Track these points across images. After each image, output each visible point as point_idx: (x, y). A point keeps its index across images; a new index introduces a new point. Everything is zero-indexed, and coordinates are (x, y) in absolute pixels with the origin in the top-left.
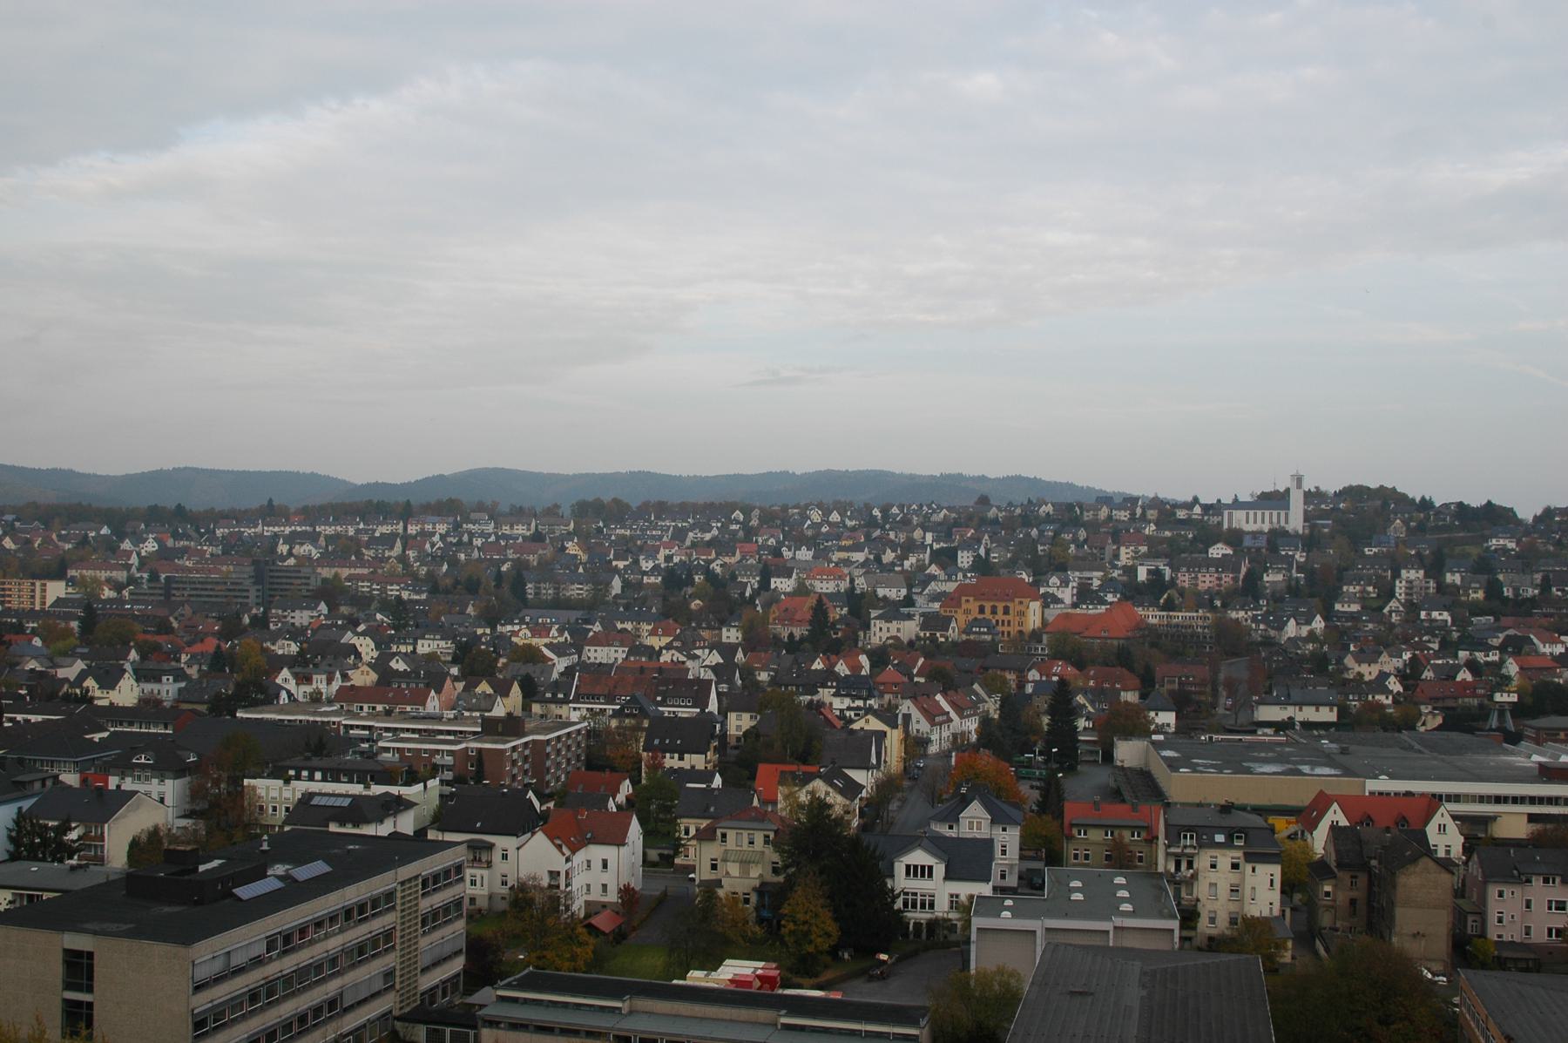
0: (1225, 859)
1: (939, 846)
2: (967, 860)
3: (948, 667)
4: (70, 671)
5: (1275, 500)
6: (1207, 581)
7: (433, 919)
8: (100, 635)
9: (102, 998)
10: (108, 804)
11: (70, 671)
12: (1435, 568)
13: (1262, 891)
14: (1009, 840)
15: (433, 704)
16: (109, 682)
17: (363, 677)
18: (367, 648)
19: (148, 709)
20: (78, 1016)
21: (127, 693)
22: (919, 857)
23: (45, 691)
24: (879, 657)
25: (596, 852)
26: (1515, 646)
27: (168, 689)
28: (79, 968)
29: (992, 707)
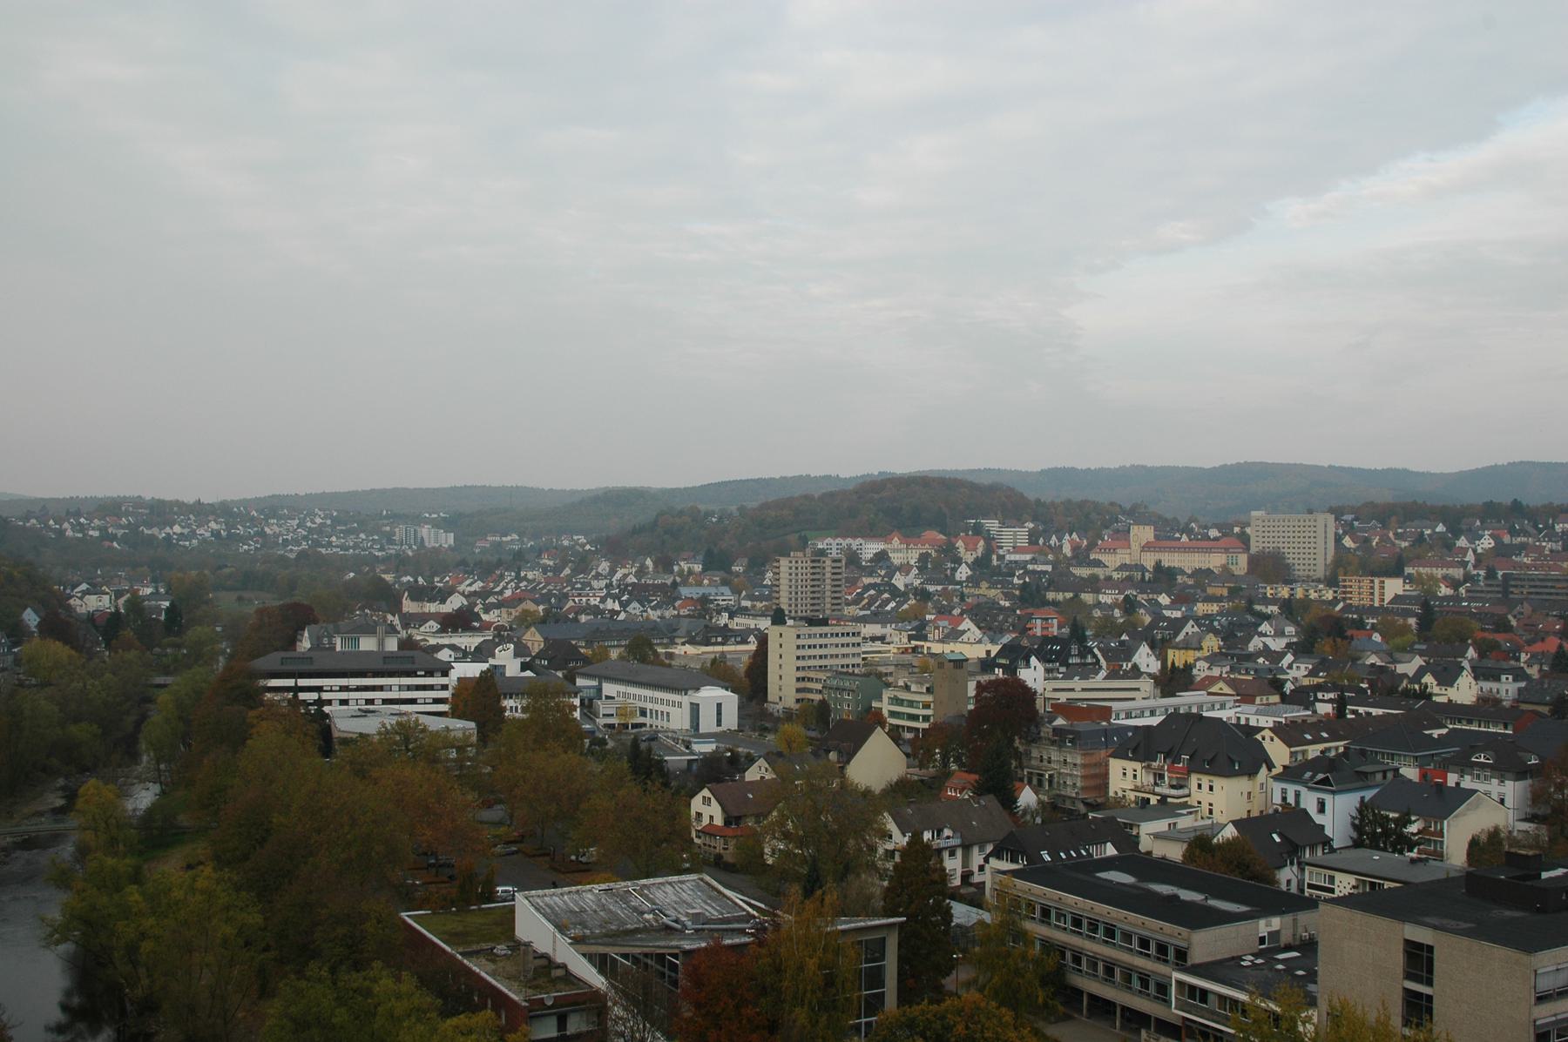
4: (1409, 667)
8: (1440, 634)
9: (1439, 991)
10: (1449, 801)
11: (1409, 667)
16: (1448, 677)
19: (1487, 707)
20: (1418, 1008)
21: (1465, 690)
23: (1385, 686)
27: (1507, 688)
28: (1419, 960)
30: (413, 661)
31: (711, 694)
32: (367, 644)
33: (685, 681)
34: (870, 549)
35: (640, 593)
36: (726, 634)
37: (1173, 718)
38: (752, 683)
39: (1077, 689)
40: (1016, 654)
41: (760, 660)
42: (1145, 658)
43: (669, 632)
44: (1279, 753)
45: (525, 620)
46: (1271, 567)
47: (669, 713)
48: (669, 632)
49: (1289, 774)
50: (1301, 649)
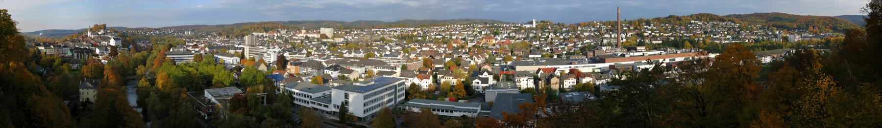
1: (480, 79)
3: (479, 50)
6: (521, 36)
7: (400, 90)
12: (555, 33)
13: (531, 84)
17: (388, 53)
18: (388, 48)
21: (353, 55)
22: (477, 80)
24: (470, 49)
25: (425, 80)
26: (566, 45)
29: (487, 56)
30: (188, 52)
32: (181, 50)
35: (224, 42)
36: (237, 48)
37: (309, 61)
38: (242, 57)
39: (294, 56)
40: (284, 51)
41: (243, 53)
46: (324, 36)
47: (228, 60)
49: (328, 68)
50: (328, 50)
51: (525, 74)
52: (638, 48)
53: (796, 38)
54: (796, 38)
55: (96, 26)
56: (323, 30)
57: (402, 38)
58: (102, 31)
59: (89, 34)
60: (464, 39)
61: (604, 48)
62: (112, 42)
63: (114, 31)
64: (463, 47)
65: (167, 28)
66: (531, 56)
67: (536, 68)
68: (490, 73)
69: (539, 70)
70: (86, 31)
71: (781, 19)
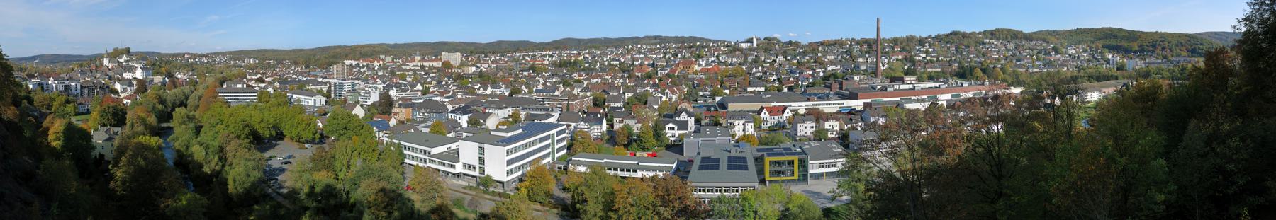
0: (742, 122)
1: (676, 123)
2: (683, 126)
3: (673, 81)
5: (750, 41)
7: (559, 141)
14: (692, 121)
15: (557, 93)
17: (540, 87)
18: (541, 81)
20: (482, 160)
21: (489, 91)
22: (671, 125)
28: (482, 150)
30: (250, 89)
31: (318, 98)
33: (311, 94)
34: (354, 63)
36: (322, 83)
40: (389, 87)
42: (419, 87)
43: (308, 82)
44: (450, 107)
45: (274, 81)
46: (447, 65)
47: (309, 101)
48: (308, 82)
49: (452, 112)
51: (742, 115)
52: (907, 78)
53: (1137, 64)
54: (1137, 64)
55: (116, 50)
56: (445, 56)
57: (562, 64)
58: (125, 58)
59: (106, 62)
60: (653, 65)
61: (856, 78)
62: (139, 74)
63: (142, 56)
64: (649, 77)
65: (218, 54)
66: (750, 89)
67: (757, 106)
68: (690, 115)
69: (762, 109)
70: (101, 57)
71: (1115, 37)
